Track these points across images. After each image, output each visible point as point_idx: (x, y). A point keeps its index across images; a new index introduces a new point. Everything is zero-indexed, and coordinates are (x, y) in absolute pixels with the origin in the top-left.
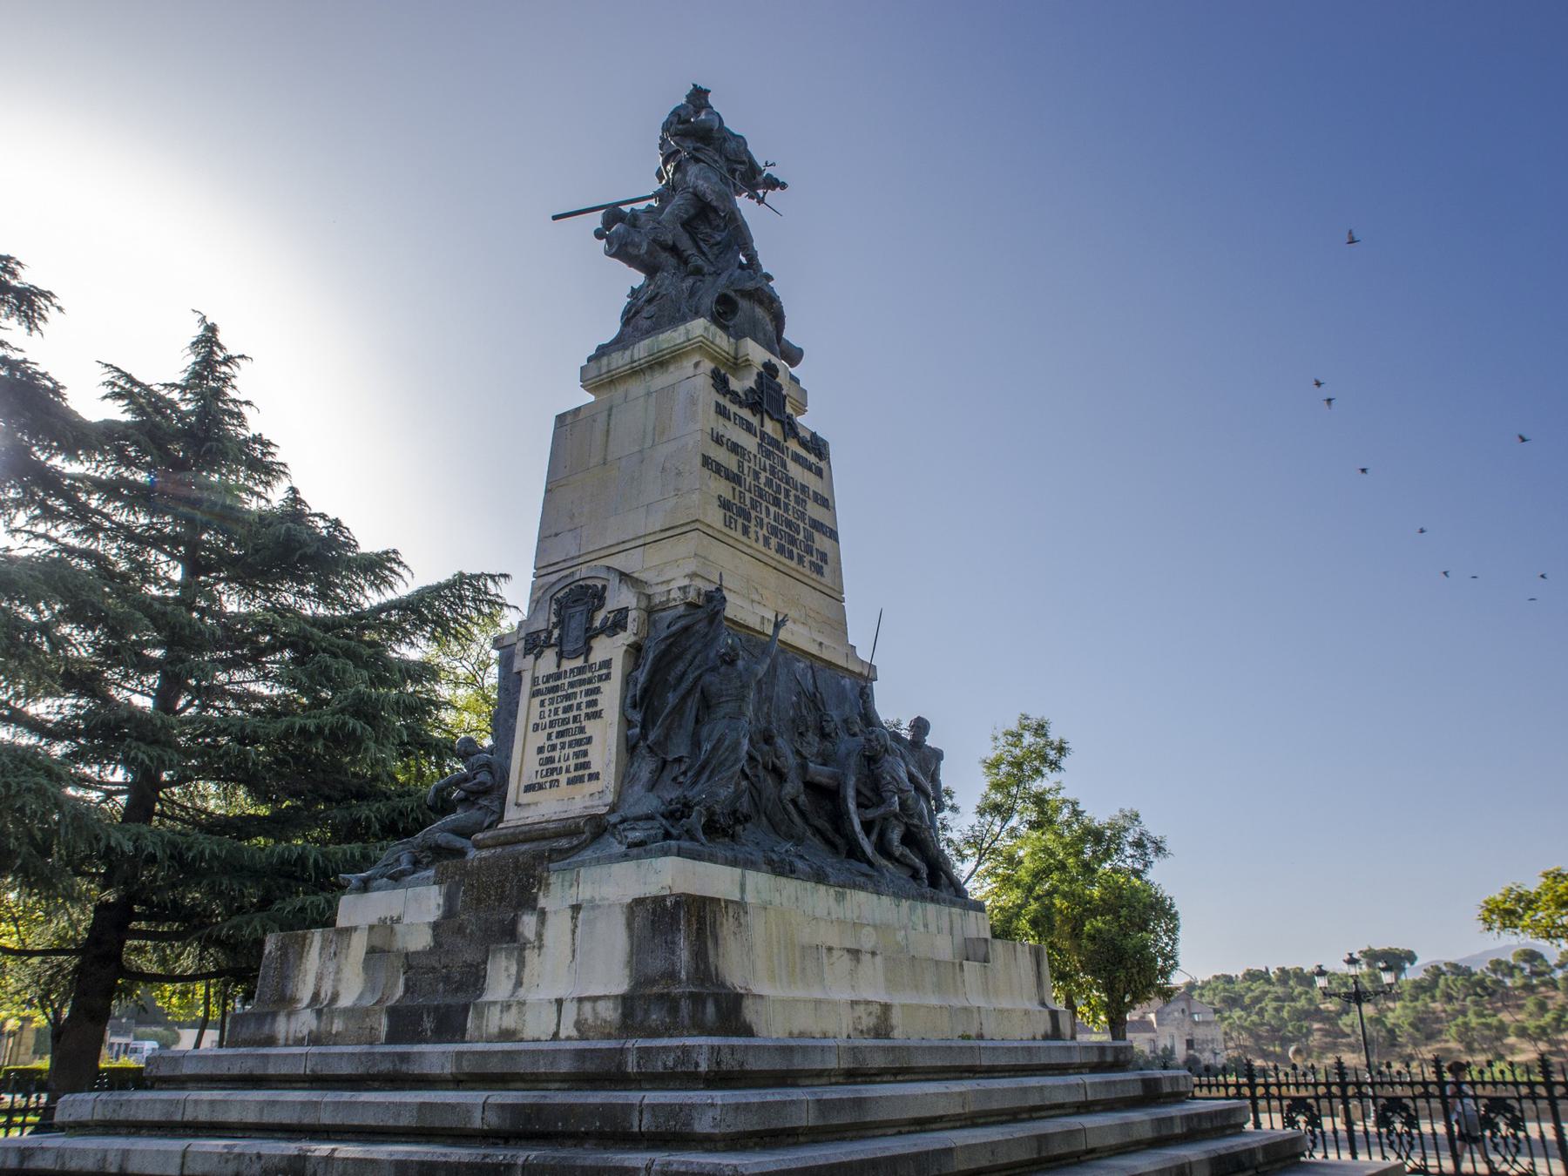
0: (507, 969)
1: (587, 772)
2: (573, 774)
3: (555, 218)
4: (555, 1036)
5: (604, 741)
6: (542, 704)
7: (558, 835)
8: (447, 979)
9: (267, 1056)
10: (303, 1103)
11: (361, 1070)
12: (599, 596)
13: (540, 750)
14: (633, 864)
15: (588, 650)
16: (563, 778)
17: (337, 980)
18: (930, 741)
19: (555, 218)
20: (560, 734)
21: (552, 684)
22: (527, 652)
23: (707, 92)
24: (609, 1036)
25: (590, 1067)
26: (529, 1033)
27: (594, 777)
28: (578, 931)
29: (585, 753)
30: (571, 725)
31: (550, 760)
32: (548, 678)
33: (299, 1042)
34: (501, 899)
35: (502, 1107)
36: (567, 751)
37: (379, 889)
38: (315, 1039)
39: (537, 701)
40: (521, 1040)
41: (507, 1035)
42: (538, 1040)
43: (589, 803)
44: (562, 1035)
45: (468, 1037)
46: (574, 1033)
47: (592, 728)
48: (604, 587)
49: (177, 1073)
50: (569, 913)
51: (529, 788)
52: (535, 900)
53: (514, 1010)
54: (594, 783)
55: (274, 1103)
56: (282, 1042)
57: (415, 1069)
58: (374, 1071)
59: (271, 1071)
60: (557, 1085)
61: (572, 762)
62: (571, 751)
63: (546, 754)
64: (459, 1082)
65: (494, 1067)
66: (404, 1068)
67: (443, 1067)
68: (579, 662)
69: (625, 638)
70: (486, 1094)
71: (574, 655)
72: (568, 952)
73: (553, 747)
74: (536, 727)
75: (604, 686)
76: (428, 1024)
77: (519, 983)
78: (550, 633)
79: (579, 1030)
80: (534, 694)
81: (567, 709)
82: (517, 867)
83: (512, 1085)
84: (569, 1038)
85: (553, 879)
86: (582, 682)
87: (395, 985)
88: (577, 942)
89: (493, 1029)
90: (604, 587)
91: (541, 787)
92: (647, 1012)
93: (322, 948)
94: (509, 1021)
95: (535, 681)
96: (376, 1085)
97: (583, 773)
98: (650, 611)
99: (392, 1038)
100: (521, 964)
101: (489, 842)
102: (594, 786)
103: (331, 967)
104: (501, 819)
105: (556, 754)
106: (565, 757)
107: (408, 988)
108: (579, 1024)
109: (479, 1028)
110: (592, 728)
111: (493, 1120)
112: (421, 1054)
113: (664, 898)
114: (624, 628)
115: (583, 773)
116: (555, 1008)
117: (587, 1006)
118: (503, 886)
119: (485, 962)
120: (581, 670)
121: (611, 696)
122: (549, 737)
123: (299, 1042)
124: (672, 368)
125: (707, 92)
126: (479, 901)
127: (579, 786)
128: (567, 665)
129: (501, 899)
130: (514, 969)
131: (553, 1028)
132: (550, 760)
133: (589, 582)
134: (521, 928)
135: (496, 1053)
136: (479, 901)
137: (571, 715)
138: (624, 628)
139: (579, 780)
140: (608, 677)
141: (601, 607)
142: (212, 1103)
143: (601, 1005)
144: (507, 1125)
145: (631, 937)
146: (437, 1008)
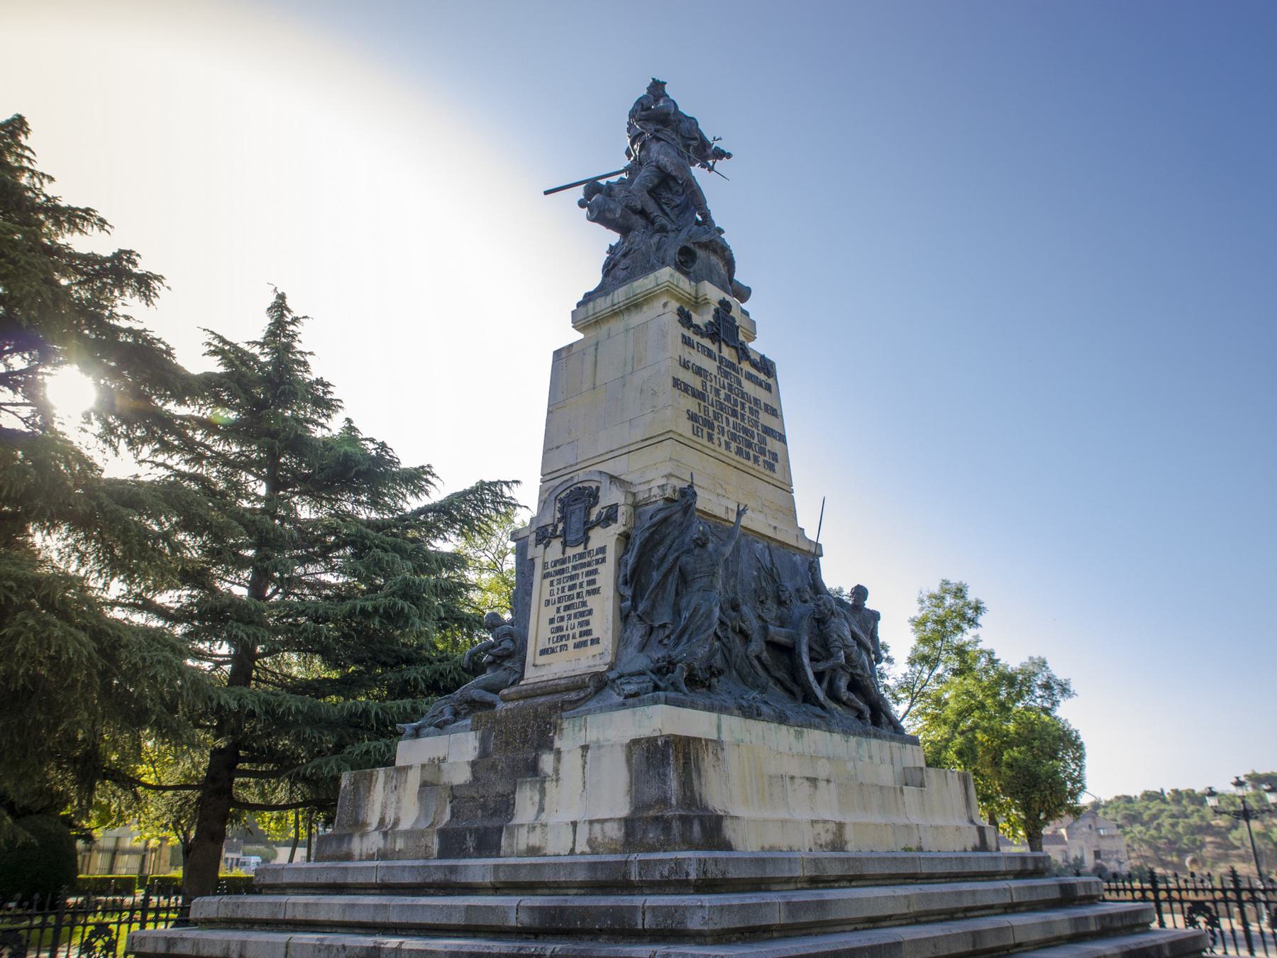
0: (531, 798)
1: (589, 638)
2: (578, 640)
3: (546, 193)
4: (572, 852)
5: (603, 611)
6: (552, 584)
7: (568, 689)
8: (484, 807)
9: (346, 869)
10: (375, 906)
11: (419, 880)
12: (593, 496)
13: (552, 621)
14: (629, 712)
15: (586, 540)
16: (571, 643)
17: (398, 808)
18: (869, 604)
19: (546, 193)
20: (567, 608)
21: (559, 567)
22: (538, 542)
24: (615, 851)
25: (601, 876)
26: (550, 849)
27: (595, 641)
28: (587, 767)
29: (587, 623)
30: (576, 600)
32: (556, 563)
33: (370, 857)
34: (524, 742)
35: (532, 909)
36: (573, 621)
37: (428, 735)
38: (383, 855)
39: (547, 581)
40: (545, 855)
41: (533, 851)
42: (559, 855)
43: (592, 663)
44: (578, 850)
45: (502, 853)
46: (587, 849)
47: (592, 602)
48: (598, 488)
49: (279, 882)
50: (580, 751)
51: (544, 652)
52: (552, 742)
53: (538, 830)
54: (595, 646)
55: (353, 906)
56: (357, 857)
57: (462, 879)
58: (429, 880)
59: (350, 880)
60: (575, 891)
61: (577, 631)
62: (576, 621)
63: (556, 624)
64: (496, 889)
65: (523, 877)
66: (453, 878)
67: (484, 876)
68: (580, 549)
69: (616, 529)
70: (519, 898)
71: (576, 543)
72: (581, 783)
73: (562, 619)
74: (548, 603)
75: (601, 567)
76: (470, 843)
77: (541, 809)
78: (556, 527)
79: (591, 847)
80: (545, 576)
81: (572, 588)
82: (536, 716)
83: (539, 891)
84: (583, 853)
85: (565, 725)
86: (583, 565)
87: (443, 812)
89: (522, 846)
90: (598, 488)
91: (553, 651)
92: (645, 832)
93: (386, 783)
94: (535, 840)
95: (545, 565)
96: (432, 891)
97: (586, 639)
98: (636, 506)
99: (443, 854)
100: (543, 792)
101: (514, 696)
102: (596, 649)
104: (522, 678)
105: (564, 624)
106: (572, 627)
107: (453, 814)
108: (591, 842)
109: (511, 845)
110: (592, 602)
111: (525, 919)
112: (466, 867)
113: (655, 739)
114: (615, 521)
115: (586, 639)
116: (571, 828)
117: (597, 827)
118: (526, 731)
119: (514, 793)
120: (581, 556)
121: (606, 576)
122: (558, 609)
123: (370, 857)
124: (645, 308)
126: (507, 743)
127: (583, 649)
128: (571, 552)
129: (524, 742)
130: (537, 798)
131: (570, 845)
132: (560, 629)
133: (586, 485)
135: (525, 865)
136: (507, 743)
137: (575, 592)
138: (615, 521)
139: (584, 644)
140: (604, 560)
141: (596, 503)
142: (306, 905)
143: (608, 826)
144: (536, 924)
145: (630, 770)
146: (477, 830)
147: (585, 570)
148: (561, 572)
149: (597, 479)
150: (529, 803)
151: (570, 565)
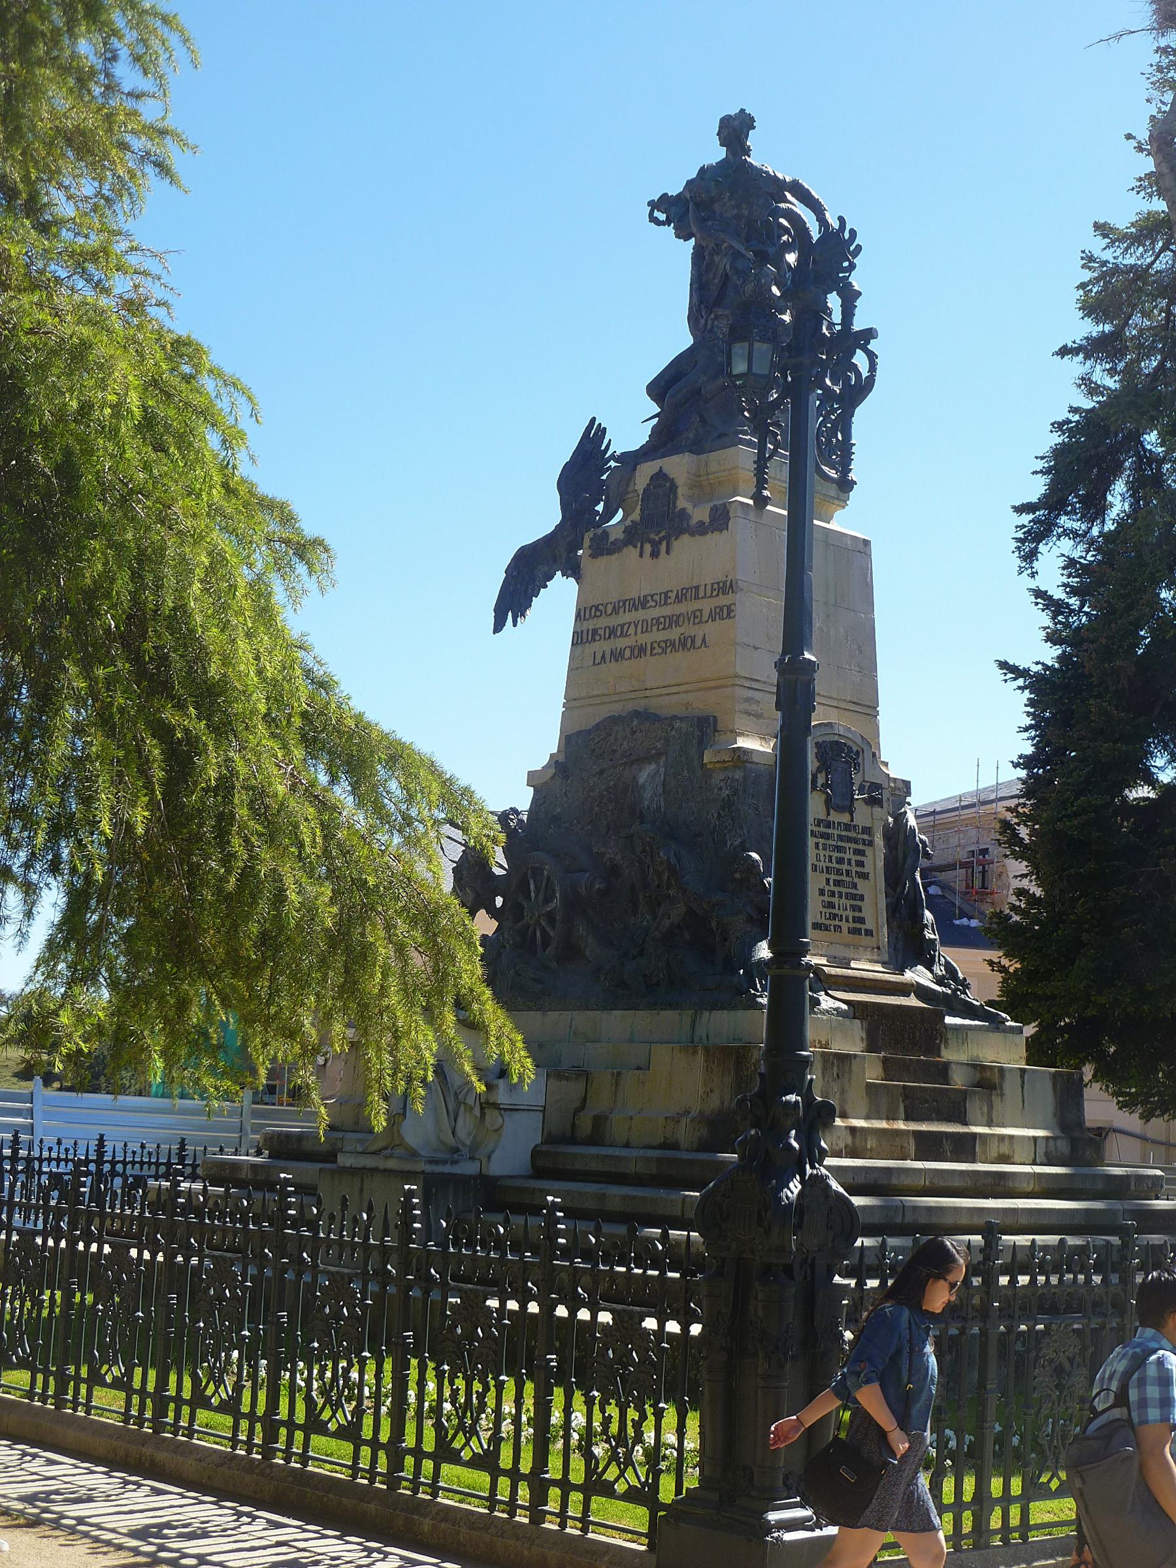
0: (981, 1109)
2: (852, 925)
16: (845, 926)
20: (838, 883)
21: (822, 829)
23: (754, 128)
27: (869, 933)
29: (860, 910)
30: (844, 878)
31: (831, 905)
62: (849, 903)
63: (826, 898)
68: (845, 818)
71: (840, 809)
81: (840, 861)
86: (850, 840)
88: (1026, 1094)
100: (991, 1107)
103: (836, 1088)
110: (863, 887)
120: (847, 827)
122: (828, 880)
125: (754, 128)
128: (835, 817)
130: (985, 1109)
133: (849, 743)
134: (950, 1073)
137: (845, 867)
140: (871, 843)
145: (1055, 1096)
147: (853, 846)
148: (826, 836)
149: (859, 741)
150: (979, 1113)
151: (836, 832)
